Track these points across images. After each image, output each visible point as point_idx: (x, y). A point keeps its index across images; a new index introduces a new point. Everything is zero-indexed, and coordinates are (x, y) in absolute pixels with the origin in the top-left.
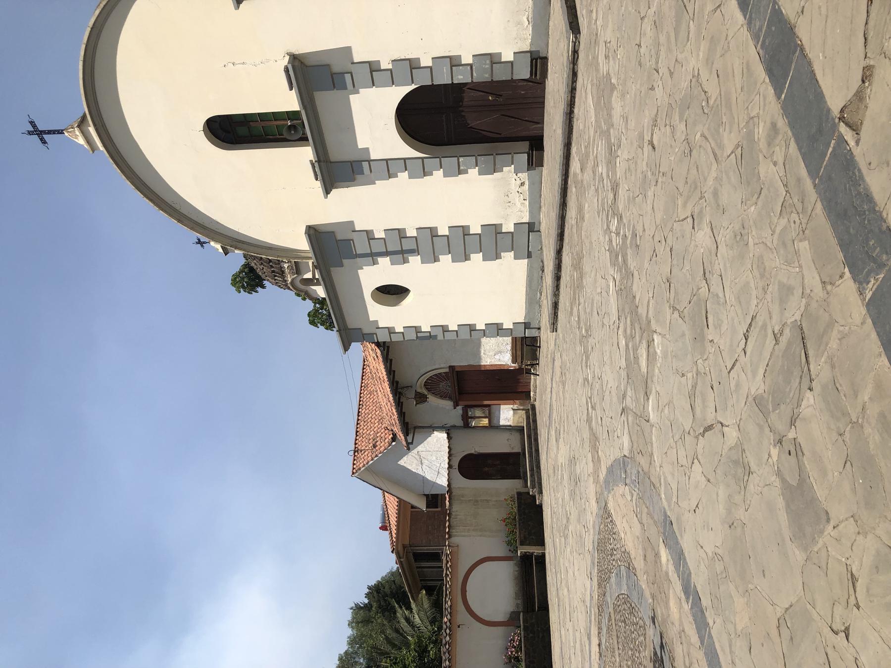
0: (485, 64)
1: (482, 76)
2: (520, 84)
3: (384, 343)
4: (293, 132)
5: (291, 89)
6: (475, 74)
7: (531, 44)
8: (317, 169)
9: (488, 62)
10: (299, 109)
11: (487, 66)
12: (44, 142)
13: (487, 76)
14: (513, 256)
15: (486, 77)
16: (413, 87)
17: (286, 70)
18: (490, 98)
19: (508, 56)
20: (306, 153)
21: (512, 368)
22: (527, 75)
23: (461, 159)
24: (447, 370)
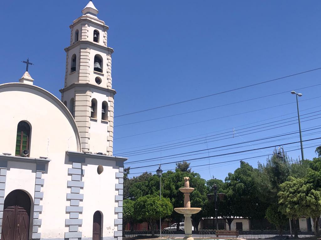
0: (39, 223)
1: (35, 222)
2: (22, 236)
4: (26, 152)
5: (41, 158)
7: (43, 239)
8: (7, 155)
9: (40, 224)
11: (38, 224)
12: (24, 62)
13: (35, 224)
15: (34, 223)
19: (40, 230)
20: (13, 154)
22: (33, 238)
23: (2, 212)
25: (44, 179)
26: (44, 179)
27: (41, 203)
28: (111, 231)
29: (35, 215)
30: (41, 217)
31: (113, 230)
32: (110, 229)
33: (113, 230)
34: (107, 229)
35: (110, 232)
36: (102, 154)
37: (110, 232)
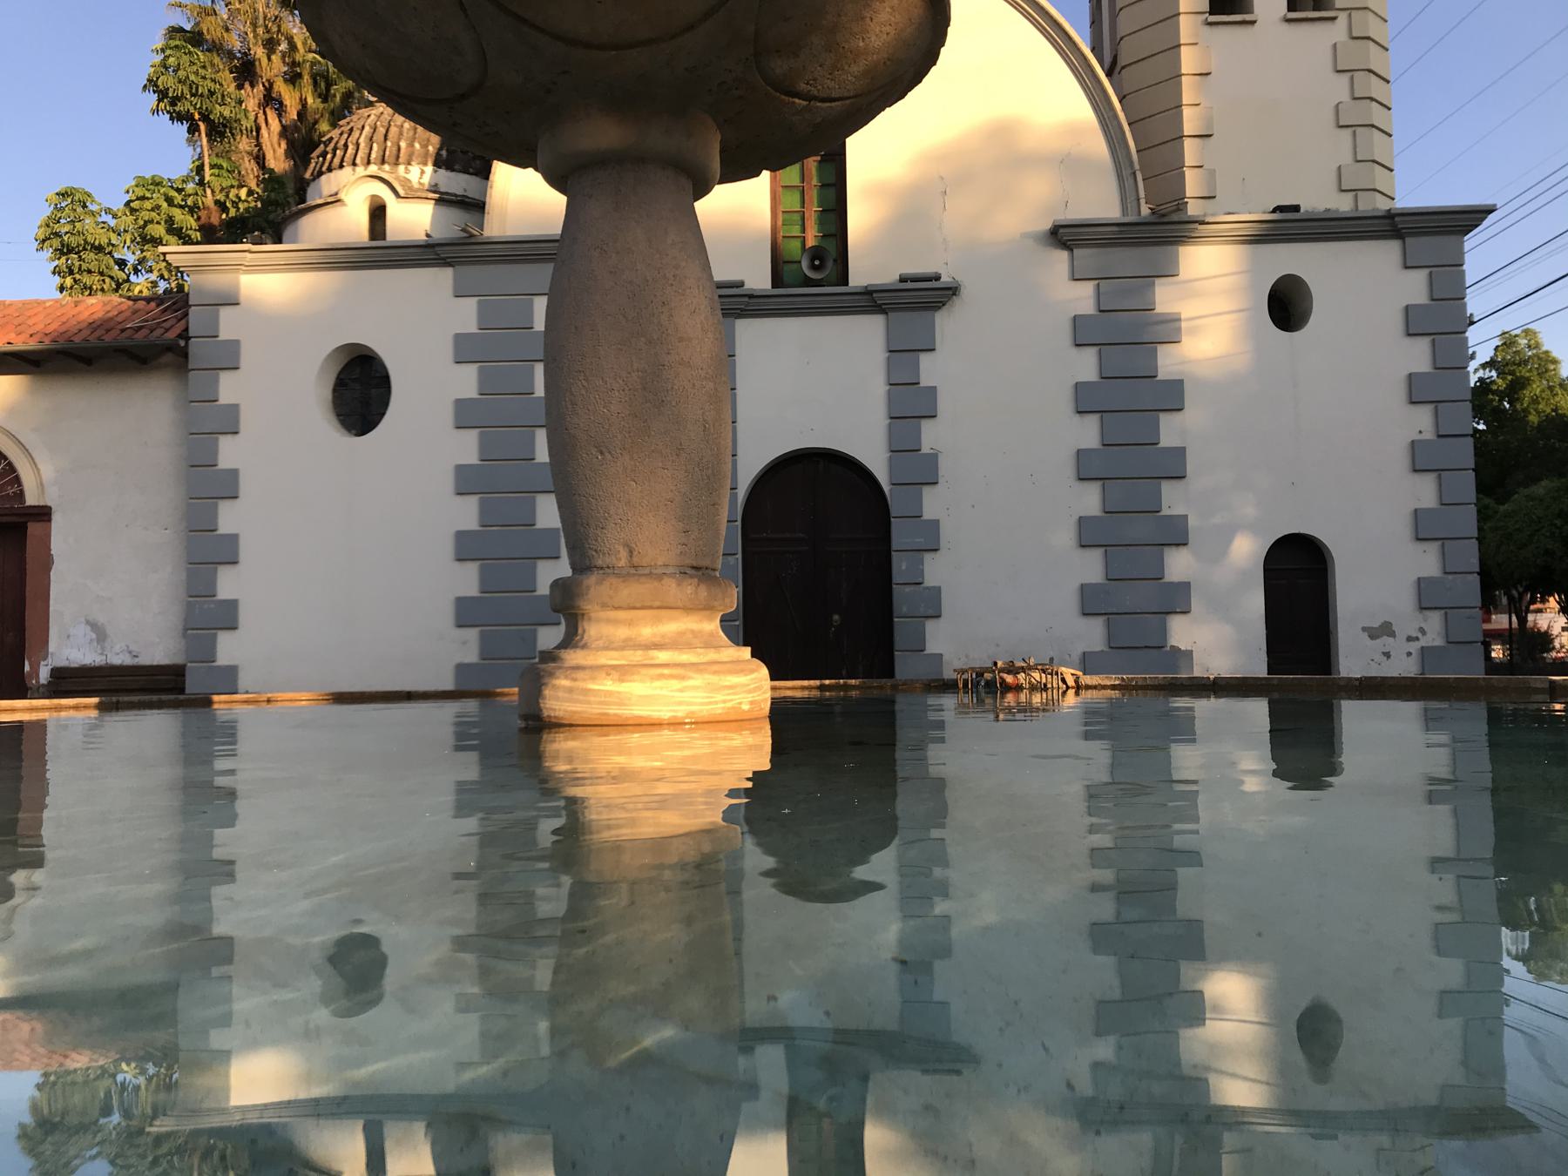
3: (185, 354)
4: (817, 263)
5: (903, 279)
6: (908, 589)
10: (850, 285)
13: (905, 609)
14: (467, 660)
16: (886, 488)
17: (937, 278)
18: (836, 617)
21: (27, 668)
24: (31, 500)
25: (933, 389)
26: (933, 389)
27: (933, 504)
28: (1397, 646)
29: (904, 567)
30: (935, 570)
31: (1410, 639)
32: (1392, 634)
33: (1410, 639)
34: (1366, 635)
35: (1387, 655)
36: (1296, 208)
37: (1387, 655)
